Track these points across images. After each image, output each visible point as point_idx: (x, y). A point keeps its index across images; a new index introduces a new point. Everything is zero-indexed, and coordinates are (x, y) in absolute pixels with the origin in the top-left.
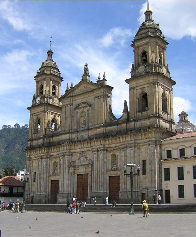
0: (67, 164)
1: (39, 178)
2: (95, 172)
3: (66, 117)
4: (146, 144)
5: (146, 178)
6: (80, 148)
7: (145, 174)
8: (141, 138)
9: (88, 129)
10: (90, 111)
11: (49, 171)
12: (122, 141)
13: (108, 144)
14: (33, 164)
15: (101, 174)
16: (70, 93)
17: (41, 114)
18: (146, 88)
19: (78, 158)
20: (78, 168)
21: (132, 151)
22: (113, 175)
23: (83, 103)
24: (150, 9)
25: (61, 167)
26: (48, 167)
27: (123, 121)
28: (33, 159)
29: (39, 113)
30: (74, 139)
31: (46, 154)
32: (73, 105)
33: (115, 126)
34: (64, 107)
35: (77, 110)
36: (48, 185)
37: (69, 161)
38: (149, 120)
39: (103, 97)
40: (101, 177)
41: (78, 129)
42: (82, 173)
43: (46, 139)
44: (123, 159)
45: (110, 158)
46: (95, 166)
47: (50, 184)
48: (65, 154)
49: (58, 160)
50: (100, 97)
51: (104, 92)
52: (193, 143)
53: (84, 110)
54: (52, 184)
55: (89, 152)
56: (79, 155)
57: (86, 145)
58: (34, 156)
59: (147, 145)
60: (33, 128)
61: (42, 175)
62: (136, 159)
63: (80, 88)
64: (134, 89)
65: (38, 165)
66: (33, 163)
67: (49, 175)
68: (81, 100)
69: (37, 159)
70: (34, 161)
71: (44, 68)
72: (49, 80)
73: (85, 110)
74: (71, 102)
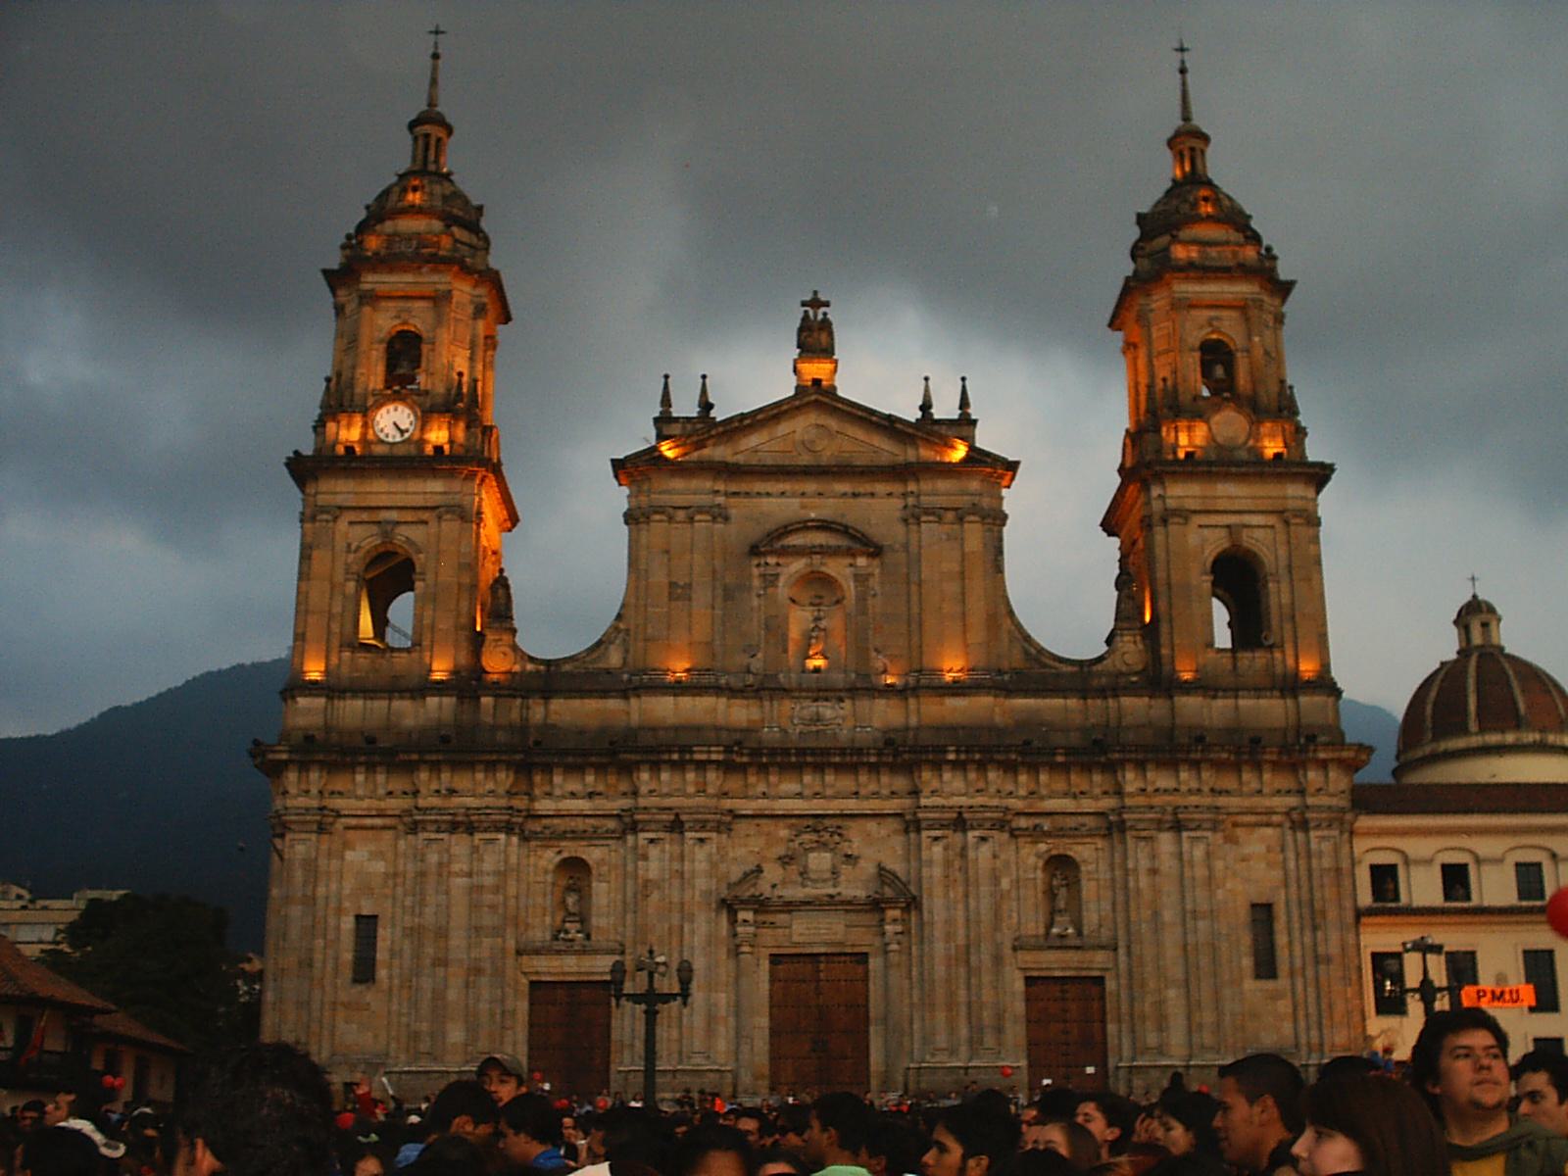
0: (701, 883)
1: (428, 962)
2: (939, 947)
3: (672, 585)
4: (1275, 818)
5: (1275, 996)
6: (799, 795)
7: (1272, 974)
8: (1269, 791)
9: (864, 688)
10: (874, 583)
11: (516, 917)
12: (1129, 788)
13: (1022, 792)
14: (342, 858)
15: (986, 958)
16: (710, 442)
17: (425, 523)
18: (1259, 534)
19: (781, 850)
20: (782, 918)
21: (1199, 852)
22: (1057, 974)
23: (824, 526)
24: (1199, 121)
25: (655, 896)
26: (512, 890)
27: (1134, 679)
28: (353, 822)
29: (409, 516)
30: (750, 730)
31: (503, 802)
32: (733, 520)
33: (1065, 698)
34: (657, 517)
35: (772, 560)
36: (514, 1012)
37: (713, 865)
38: (1290, 702)
39: (977, 518)
40: (986, 978)
41: (781, 676)
42: (816, 950)
43: (487, 701)
44: (1144, 882)
45: (1040, 874)
46: (936, 905)
47: (523, 1006)
48: (684, 818)
49: (593, 854)
50: (950, 516)
51: (981, 495)
52: (1510, 841)
53: (823, 569)
54: (531, 1004)
55: (872, 826)
56: (784, 833)
57: (846, 783)
58: (366, 803)
59: (1279, 825)
60: (337, 609)
61: (457, 941)
62: (1220, 893)
63: (784, 428)
64: (1187, 519)
65: (422, 874)
66: (347, 845)
67: (517, 942)
68: (797, 500)
69: (384, 828)
70: (351, 834)
71: (437, 225)
72: (470, 309)
73: (837, 568)
74: (720, 500)
